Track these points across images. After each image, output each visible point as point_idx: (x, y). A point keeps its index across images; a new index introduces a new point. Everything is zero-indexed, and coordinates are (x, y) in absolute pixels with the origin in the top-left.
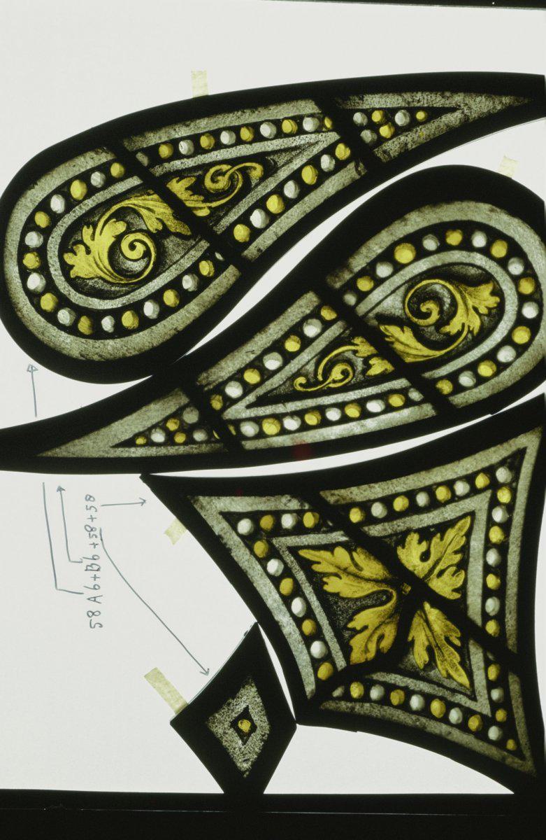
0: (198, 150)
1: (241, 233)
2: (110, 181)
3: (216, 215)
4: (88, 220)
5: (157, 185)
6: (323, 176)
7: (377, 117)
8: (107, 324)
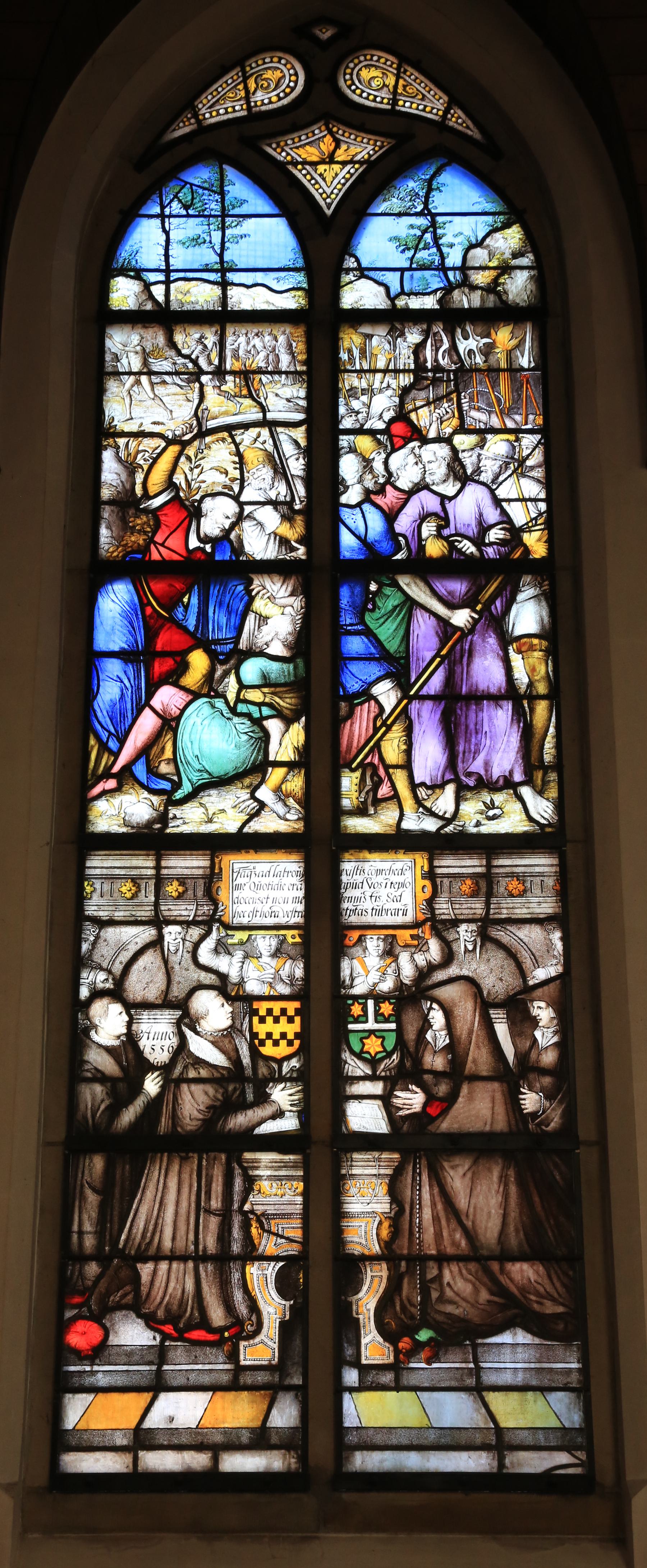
0: (415, 81)
1: (401, 103)
2: (391, 66)
3: (401, 94)
4: (377, 67)
5: (398, 77)
6: (431, 112)
7: (456, 115)
8: (353, 87)
